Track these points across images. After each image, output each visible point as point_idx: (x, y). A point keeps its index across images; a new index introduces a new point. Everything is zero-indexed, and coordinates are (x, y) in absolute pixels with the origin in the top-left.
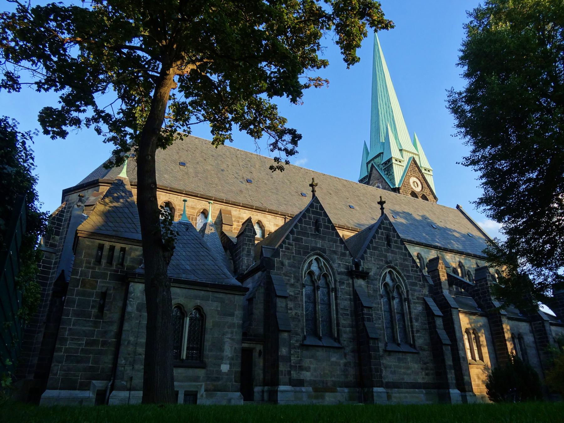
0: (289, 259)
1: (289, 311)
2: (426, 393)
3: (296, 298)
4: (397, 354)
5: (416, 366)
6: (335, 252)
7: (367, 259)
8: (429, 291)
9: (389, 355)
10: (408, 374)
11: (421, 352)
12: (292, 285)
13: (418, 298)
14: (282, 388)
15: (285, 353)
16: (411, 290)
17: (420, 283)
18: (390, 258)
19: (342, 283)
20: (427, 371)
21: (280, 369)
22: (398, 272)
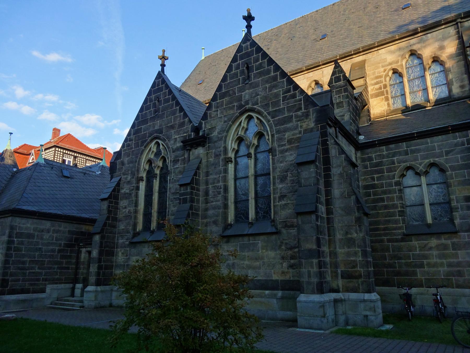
0: (128, 156)
1: (124, 210)
2: (282, 298)
3: (130, 194)
4: (240, 239)
5: (272, 254)
6: (172, 127)
7: (210, 116)
8: (317, 121)
9: (228, 242)
10: (254, 268)
11: (284, 231)
12: (129, 182)
13: (290, 142)
14: (89, 288)
15: (95, 255)
16: (278, 132)
17: (299, 113)
18: (247, 97)
19: (175, 161)
20: (292, 261)
21: (90, 270)
22: (259, 113)
